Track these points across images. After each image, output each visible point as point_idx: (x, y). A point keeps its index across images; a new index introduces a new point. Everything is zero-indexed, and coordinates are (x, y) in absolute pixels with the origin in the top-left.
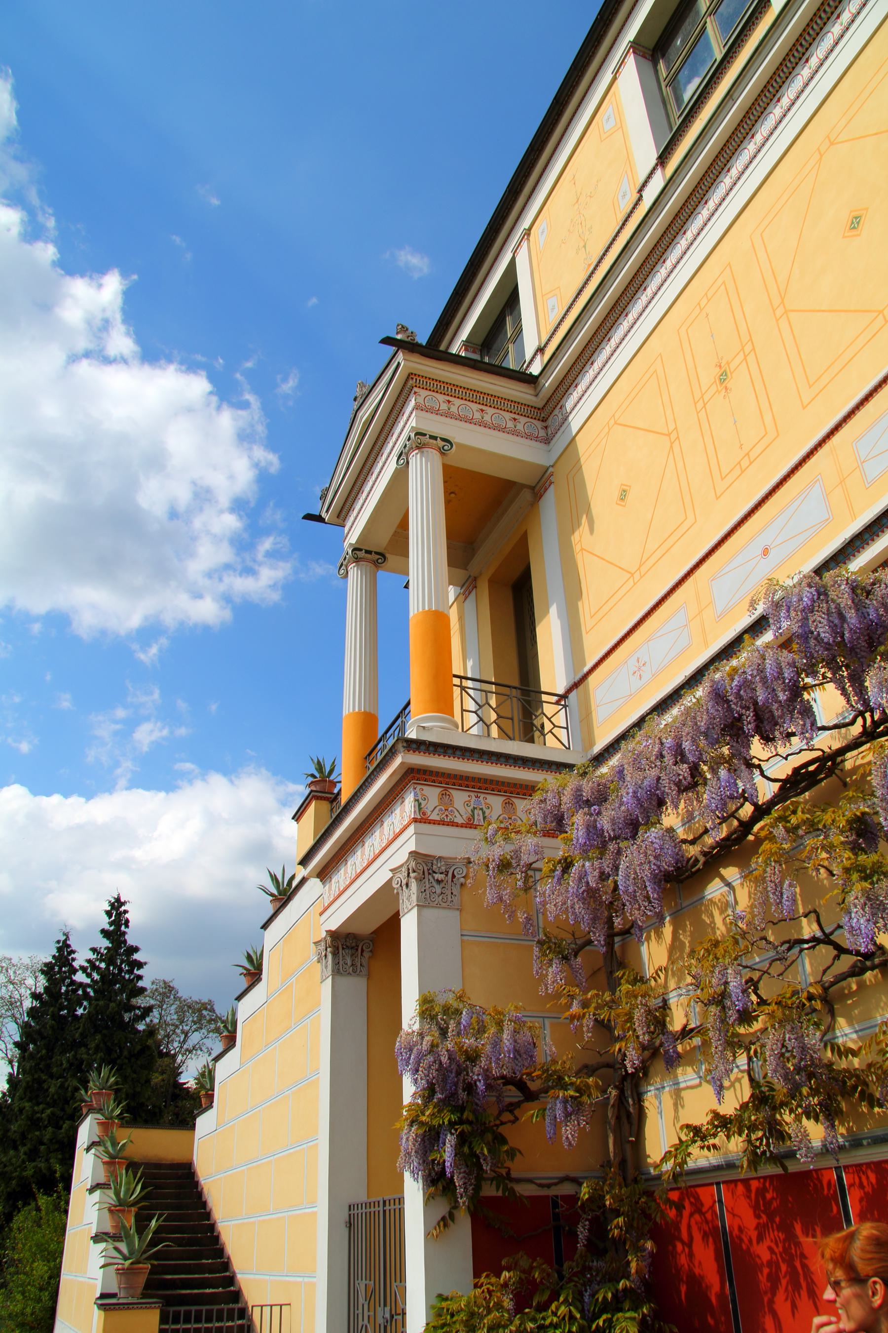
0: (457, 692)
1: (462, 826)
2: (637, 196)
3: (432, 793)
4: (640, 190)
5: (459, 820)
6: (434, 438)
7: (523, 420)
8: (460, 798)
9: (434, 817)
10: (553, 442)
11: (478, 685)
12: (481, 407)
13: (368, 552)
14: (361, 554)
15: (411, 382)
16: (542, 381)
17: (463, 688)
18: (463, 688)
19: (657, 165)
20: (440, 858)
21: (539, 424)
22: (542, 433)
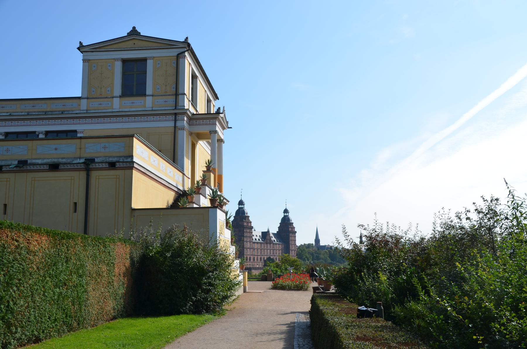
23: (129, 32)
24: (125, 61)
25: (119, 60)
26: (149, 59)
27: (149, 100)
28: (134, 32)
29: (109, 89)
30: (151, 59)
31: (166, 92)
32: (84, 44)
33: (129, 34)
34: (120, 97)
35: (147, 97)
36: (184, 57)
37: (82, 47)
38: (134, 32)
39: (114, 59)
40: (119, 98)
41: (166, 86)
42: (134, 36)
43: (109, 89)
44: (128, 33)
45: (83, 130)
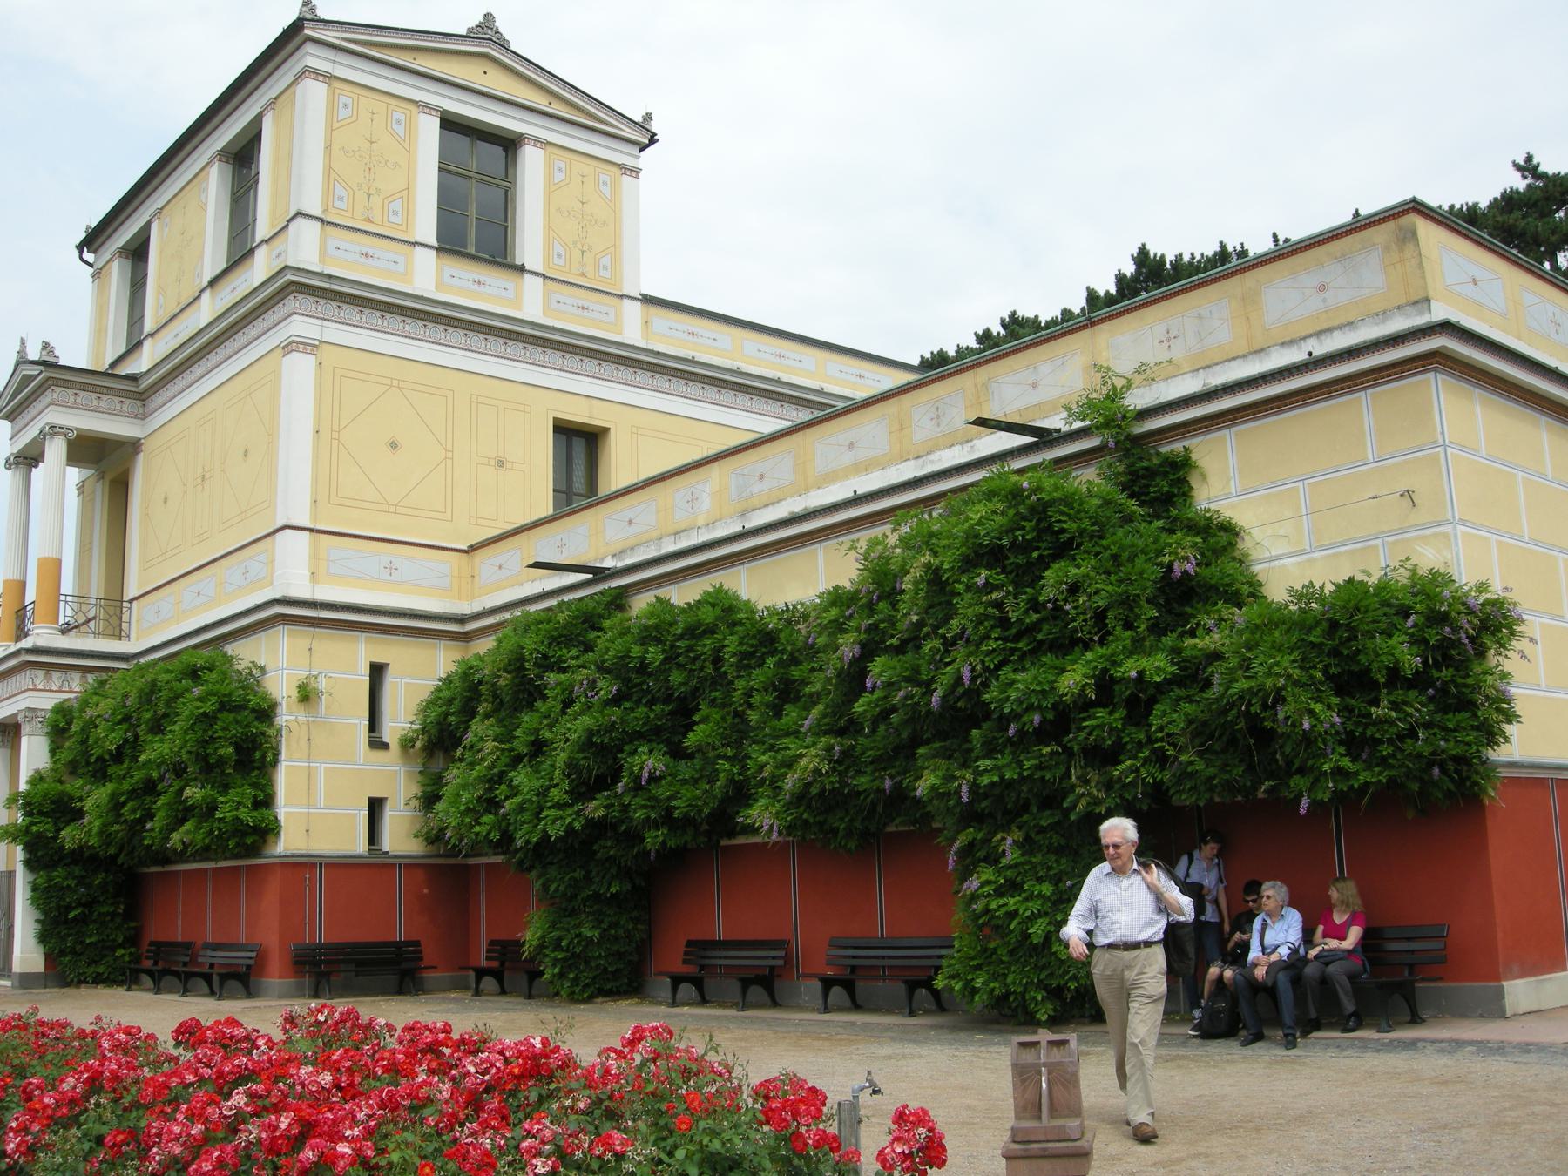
0: (62, 604)
1: (56, 691)
2: (197, 294)
3: (41, 673)
4: (202, 291)
5: (54, 688)
6: (61, 428)
7: (128, 401)
8: (56, 675)
9: (41, 687)
10: (148, 419)
11: (76, 599)
12: (98, 395)
13: (25, 458)
14: (20, 460)
15: (50, 382)
16: (140, 382)
17: (66, 602)
18: (66, 602)
19: (206, 288)
20: (42, 710)
21: (139, 403)
22: (141, 410)
23: (473, 24)
24: (450, 124)
25: (434, 113)
26: (532, 142)
27: (532, 284)
28: (486, 31)
29: (397, 206)
30: (538, 145)
31: (583, 275)
32: (323, 14)
33: (475, 35)
34: (440, 250)
35: (527, 276)
36: (634, 174)
37: (313, 20)
38: (486, 31)
39: (417, 102)
40: (434, 252)
41: (583, 252)
42: (489, 47)
43: (397, 206)
44: (470, 30)
45: (317, 343)
